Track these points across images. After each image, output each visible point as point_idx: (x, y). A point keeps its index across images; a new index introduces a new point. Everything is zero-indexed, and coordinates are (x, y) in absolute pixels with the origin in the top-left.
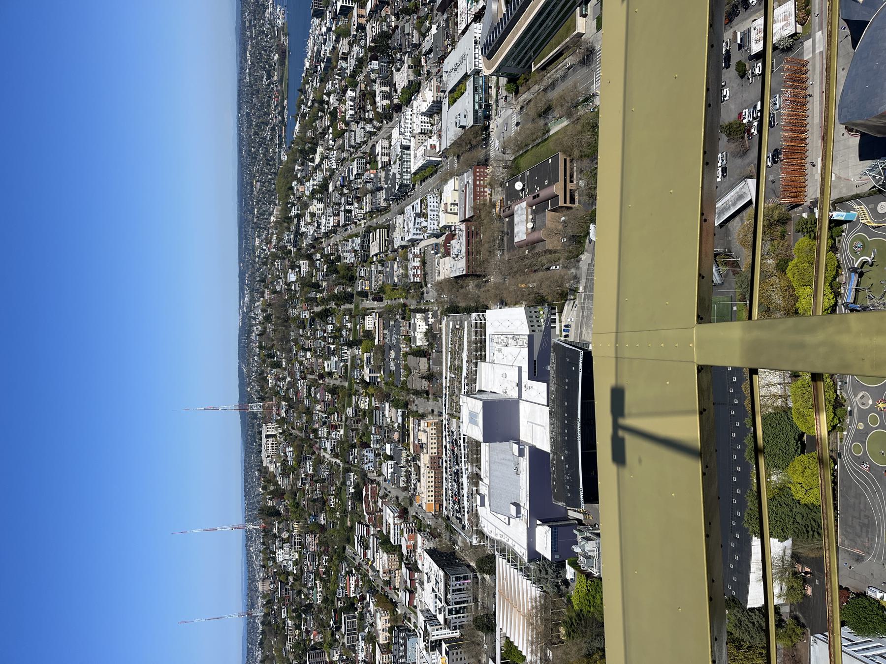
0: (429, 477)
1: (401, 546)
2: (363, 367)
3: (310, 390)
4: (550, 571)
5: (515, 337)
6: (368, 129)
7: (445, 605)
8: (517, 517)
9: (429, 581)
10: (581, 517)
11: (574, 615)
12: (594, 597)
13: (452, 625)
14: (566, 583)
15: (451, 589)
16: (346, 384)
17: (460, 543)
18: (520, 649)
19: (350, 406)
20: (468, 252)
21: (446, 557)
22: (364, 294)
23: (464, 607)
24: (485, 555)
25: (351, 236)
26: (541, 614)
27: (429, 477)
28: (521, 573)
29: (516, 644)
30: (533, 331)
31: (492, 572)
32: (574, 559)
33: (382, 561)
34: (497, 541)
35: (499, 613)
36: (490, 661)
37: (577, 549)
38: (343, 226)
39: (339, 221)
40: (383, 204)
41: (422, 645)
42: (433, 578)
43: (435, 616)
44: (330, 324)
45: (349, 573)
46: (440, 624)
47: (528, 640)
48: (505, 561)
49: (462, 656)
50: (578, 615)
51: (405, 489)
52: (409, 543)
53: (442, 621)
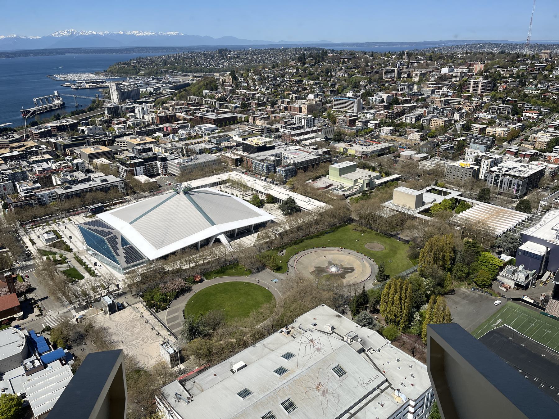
1: (551, 152)
4: (511, 245)
7: (503, 173)
8: (557, 236)
9: (522, 166)
10: (544, 279)
11: (479, 250)
12: (486, 266)
13: (488, 175)
14: (500, 253)
15: (513, 179)
17: (543, 193)
18: (464, 212)
21: (536, 181)
23: (498, 185)
24: (531, 207)
26: (483, 231)
28: (513, 226)
29: (467, 210)
31: (518, 208)
32: (514, 264)
33: (544, 138)
34: (541, 218)
35: (490, 206)
36: (460, 193)
37: (521, 267)
41: (480, 154)
42: (524, 169)
43: (497, 165)
45: (540, 114)
46: (490, 168)
47: (469, 218)
48: (524, 219)
49: (467, 177)
50: (478, 252)
52: (553, 158)
53: (492, 169)
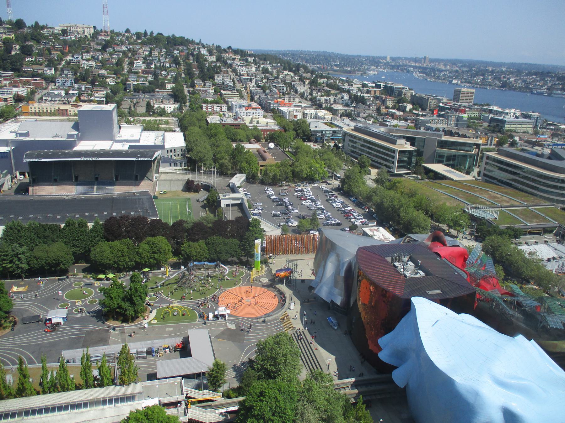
0: (51, 108)
2: (137, 81)
3: (119, 52)
5: (164, 143)
6: (306, 92)
16: (125, 71)
19: (108, 73)
20: (224, 125)
22: (193, 86)
25: (233, 81)
27: (51, 108)
30: (168, 151)
38: (240, 79)
39: (244, 76)
40: (256, 98)
44: (170, 66)
51: (41, 99)
